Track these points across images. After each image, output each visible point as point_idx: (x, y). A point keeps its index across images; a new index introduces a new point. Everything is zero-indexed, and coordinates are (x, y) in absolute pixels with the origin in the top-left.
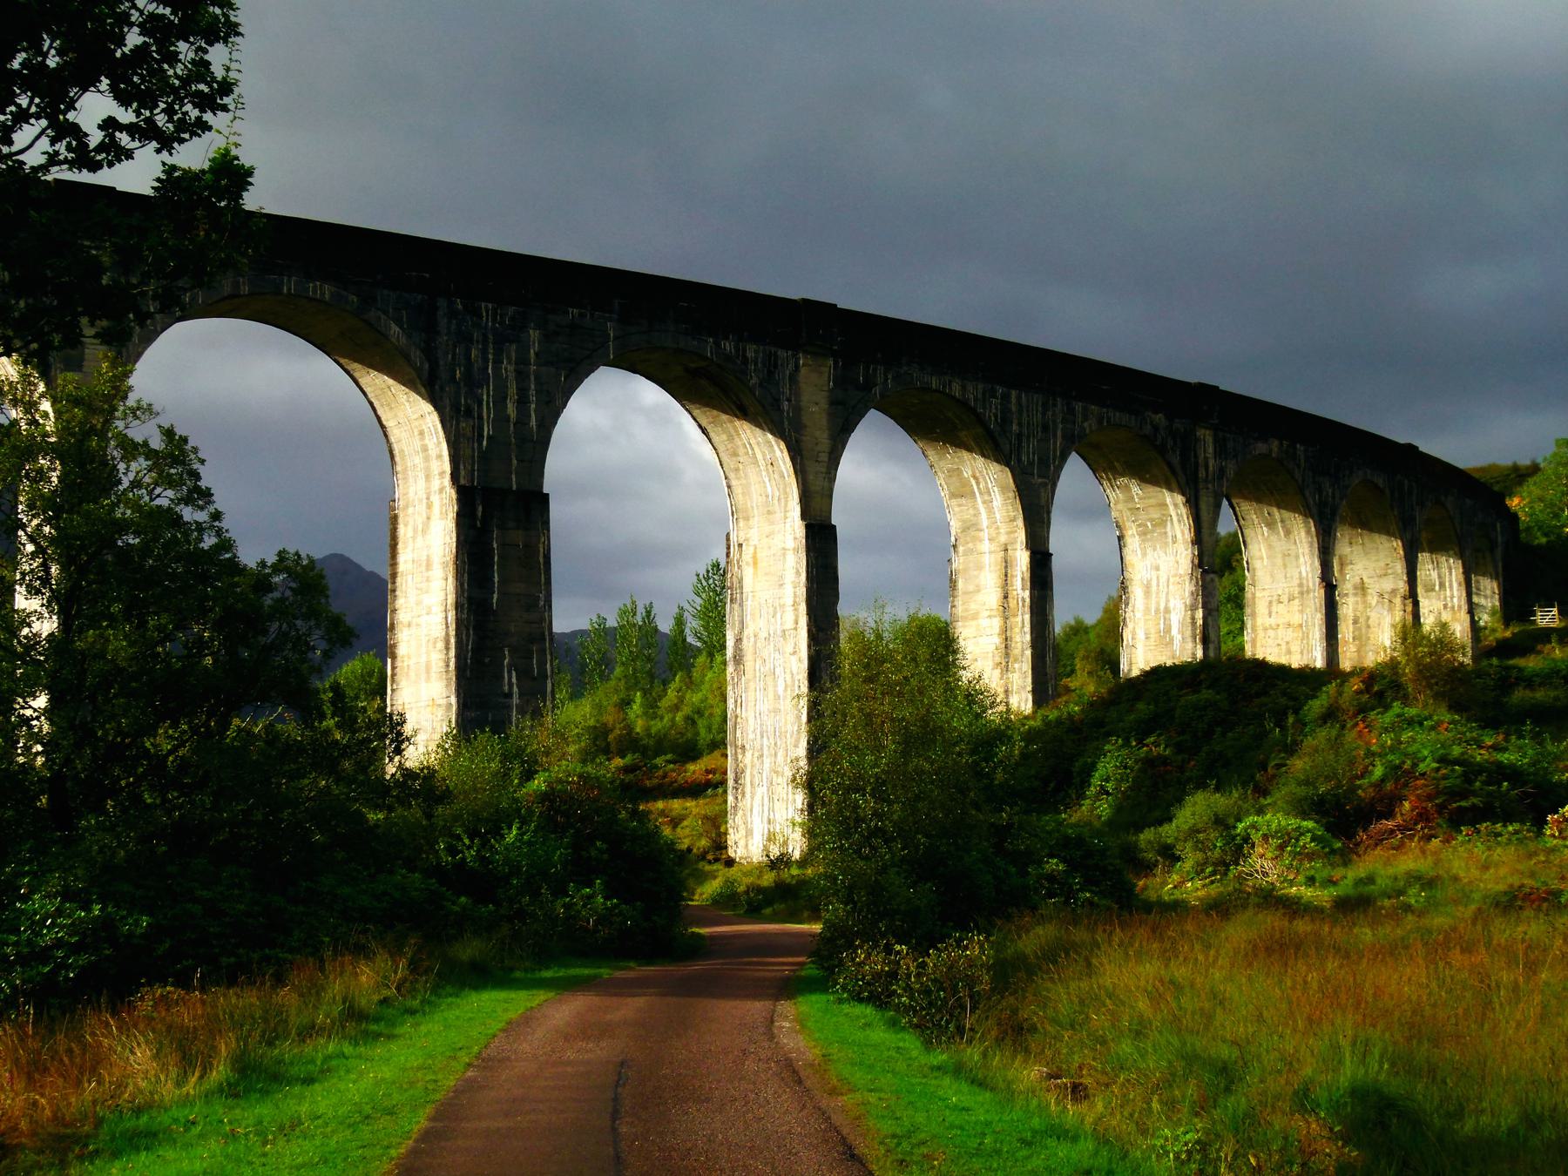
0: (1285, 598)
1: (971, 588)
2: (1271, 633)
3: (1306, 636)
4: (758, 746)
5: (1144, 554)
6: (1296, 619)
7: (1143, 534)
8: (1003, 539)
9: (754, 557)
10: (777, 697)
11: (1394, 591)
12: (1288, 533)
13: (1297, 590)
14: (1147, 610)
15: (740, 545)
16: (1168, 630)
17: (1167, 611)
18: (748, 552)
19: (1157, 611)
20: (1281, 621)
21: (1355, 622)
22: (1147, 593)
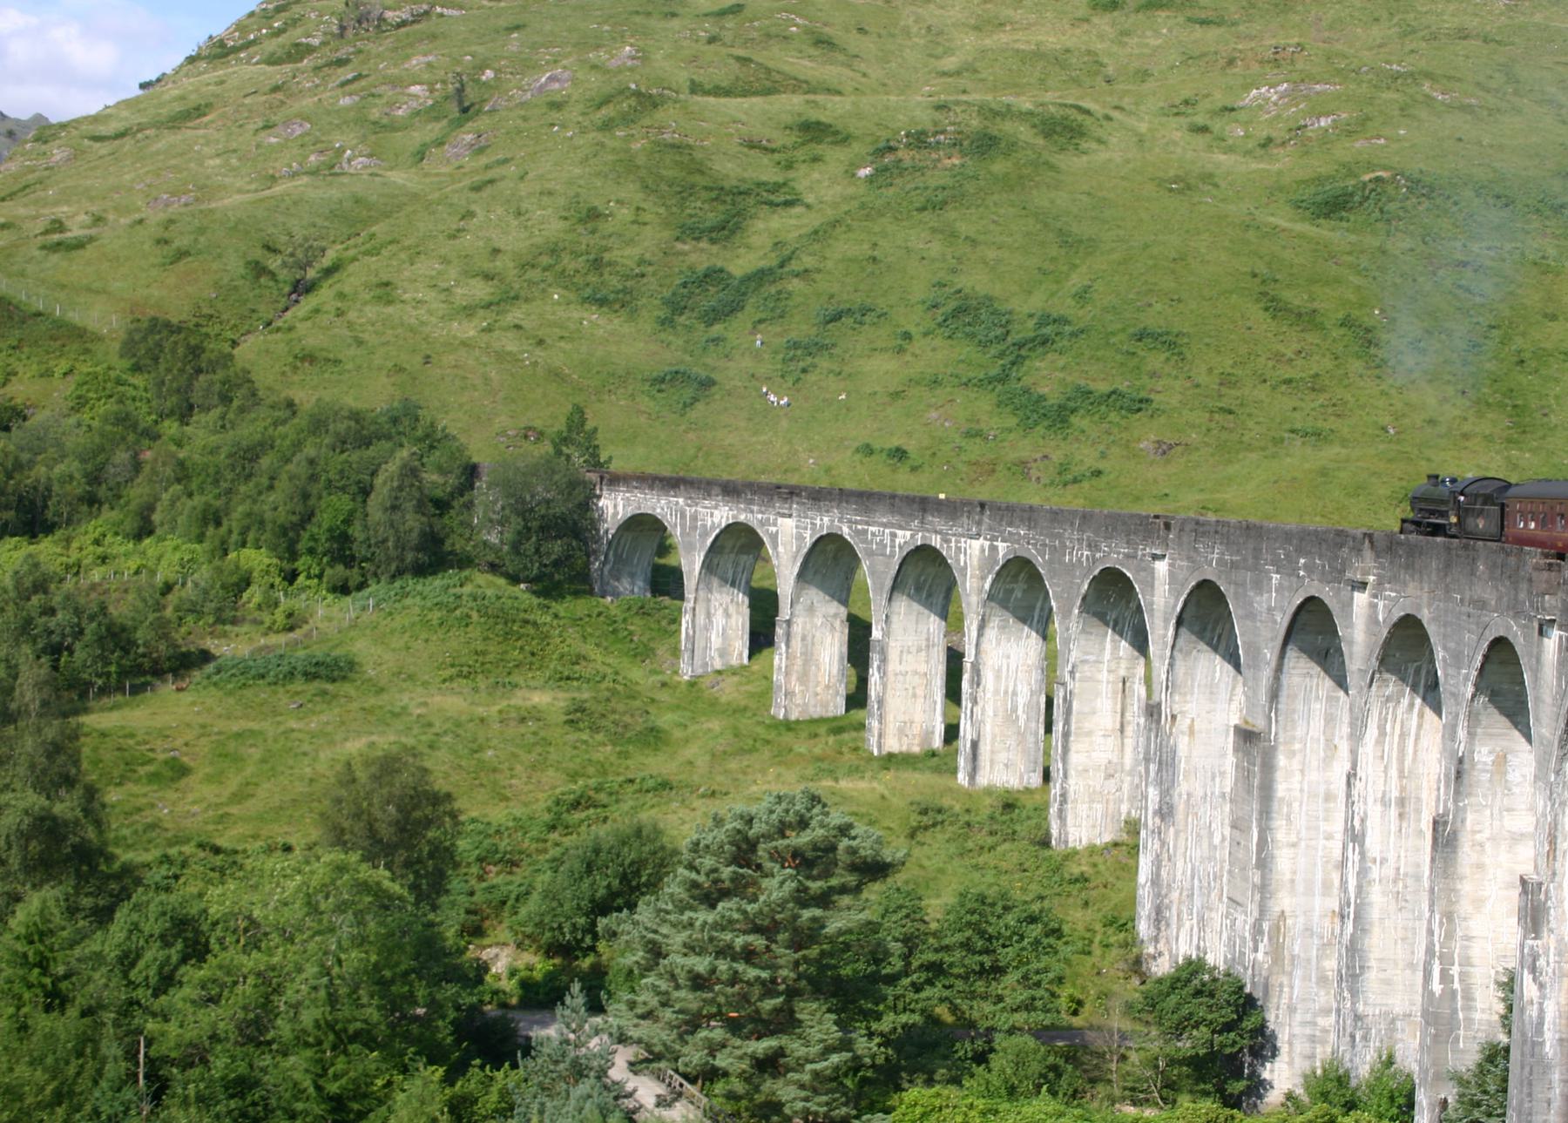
0: (914, 650)
1: (1086, 710)
2: (901, 678)
3: (928, 684)
4: (1187, 885)
5: (998, 643)
6: (923, 668)
7: (1002, 628)
8: (1122, 673)
9: (1191, 727)
10: (1212, 847)
11: (836, 616)
12: (929, 595)
13: (924, 644)
14: (997, 692)
15: (1174, 717)
16: (1014, 709)
17: (1015, 693)
18: (1183, 724)
19: (1006, 692)
20: (909, 669)
21: (804, 639)
22: (998, 677)
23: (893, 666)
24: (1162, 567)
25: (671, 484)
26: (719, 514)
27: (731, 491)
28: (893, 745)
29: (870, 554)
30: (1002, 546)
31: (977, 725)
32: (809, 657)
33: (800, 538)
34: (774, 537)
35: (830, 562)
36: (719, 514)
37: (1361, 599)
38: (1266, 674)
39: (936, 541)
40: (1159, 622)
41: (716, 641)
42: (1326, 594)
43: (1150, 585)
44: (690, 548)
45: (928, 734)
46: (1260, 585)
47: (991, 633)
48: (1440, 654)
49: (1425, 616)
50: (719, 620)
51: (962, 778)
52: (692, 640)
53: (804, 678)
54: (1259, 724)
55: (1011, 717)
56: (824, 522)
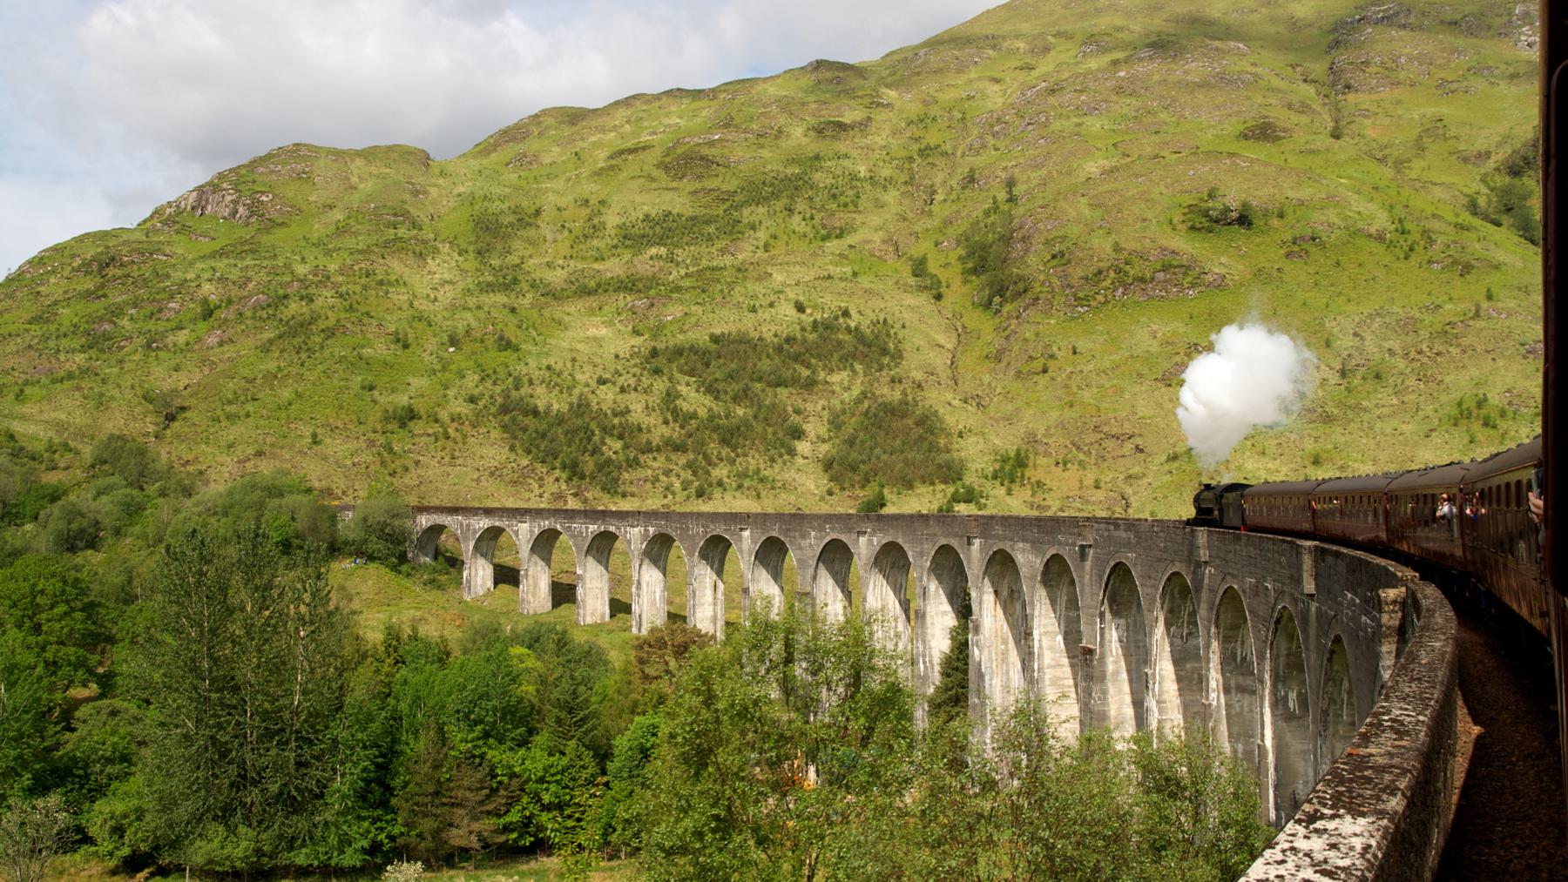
23: (588, 585)
24: (746, 534)
25: (454, 510)
26: (484, 523)
27: (488, 512)
28: (589, 620)
29: (574, 537)
30: (651, 530)
31: (641, 606)
32: (536, 585)
33: (532, 532)
34: (517, 533)
35: (545, 544)
36: (484, 523)
37: (863, 540)
38: (811, 571)
39: (612, 529)
40: (746, 555)
41: (479, 581)
42: (844, 538)
43: (740, 539)
44: (467, 540)
45: (603, 615)
46: (804, 536)
47: (644, 567)
48: (910, 554)
49: (900, 541)
50: (481, 573)
51: (634, 630)
52: (469, 581)
53: (534, 595)
54: (808, 589)
55: (653, 603)
56: (546, 524)
